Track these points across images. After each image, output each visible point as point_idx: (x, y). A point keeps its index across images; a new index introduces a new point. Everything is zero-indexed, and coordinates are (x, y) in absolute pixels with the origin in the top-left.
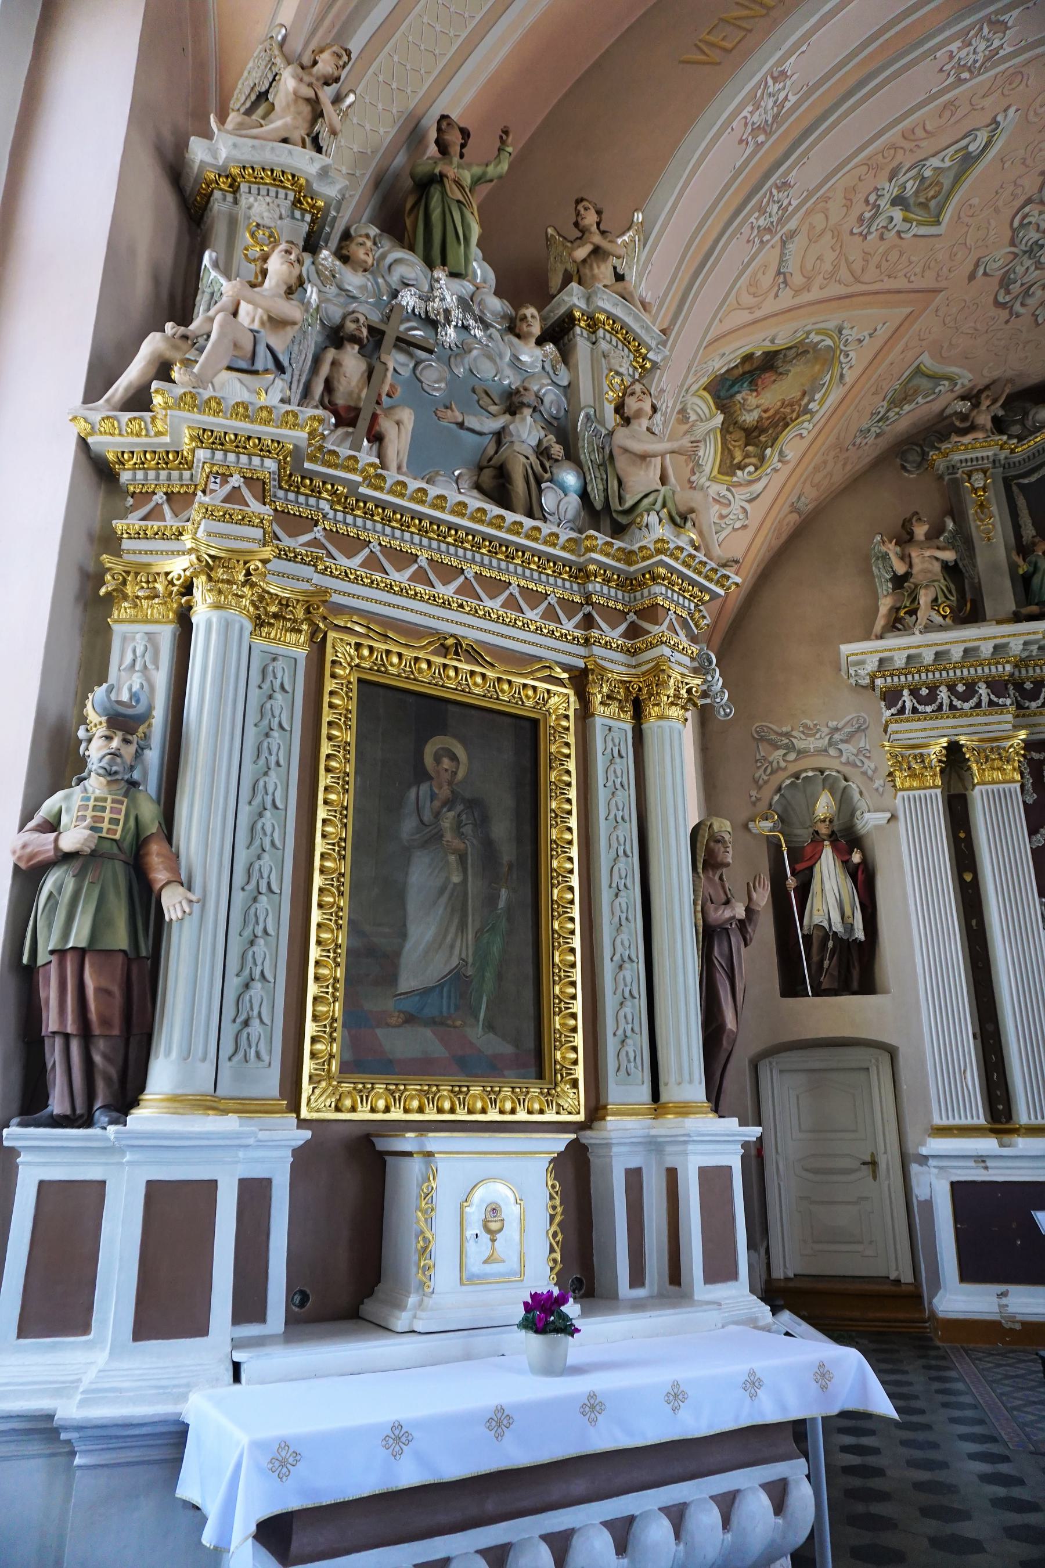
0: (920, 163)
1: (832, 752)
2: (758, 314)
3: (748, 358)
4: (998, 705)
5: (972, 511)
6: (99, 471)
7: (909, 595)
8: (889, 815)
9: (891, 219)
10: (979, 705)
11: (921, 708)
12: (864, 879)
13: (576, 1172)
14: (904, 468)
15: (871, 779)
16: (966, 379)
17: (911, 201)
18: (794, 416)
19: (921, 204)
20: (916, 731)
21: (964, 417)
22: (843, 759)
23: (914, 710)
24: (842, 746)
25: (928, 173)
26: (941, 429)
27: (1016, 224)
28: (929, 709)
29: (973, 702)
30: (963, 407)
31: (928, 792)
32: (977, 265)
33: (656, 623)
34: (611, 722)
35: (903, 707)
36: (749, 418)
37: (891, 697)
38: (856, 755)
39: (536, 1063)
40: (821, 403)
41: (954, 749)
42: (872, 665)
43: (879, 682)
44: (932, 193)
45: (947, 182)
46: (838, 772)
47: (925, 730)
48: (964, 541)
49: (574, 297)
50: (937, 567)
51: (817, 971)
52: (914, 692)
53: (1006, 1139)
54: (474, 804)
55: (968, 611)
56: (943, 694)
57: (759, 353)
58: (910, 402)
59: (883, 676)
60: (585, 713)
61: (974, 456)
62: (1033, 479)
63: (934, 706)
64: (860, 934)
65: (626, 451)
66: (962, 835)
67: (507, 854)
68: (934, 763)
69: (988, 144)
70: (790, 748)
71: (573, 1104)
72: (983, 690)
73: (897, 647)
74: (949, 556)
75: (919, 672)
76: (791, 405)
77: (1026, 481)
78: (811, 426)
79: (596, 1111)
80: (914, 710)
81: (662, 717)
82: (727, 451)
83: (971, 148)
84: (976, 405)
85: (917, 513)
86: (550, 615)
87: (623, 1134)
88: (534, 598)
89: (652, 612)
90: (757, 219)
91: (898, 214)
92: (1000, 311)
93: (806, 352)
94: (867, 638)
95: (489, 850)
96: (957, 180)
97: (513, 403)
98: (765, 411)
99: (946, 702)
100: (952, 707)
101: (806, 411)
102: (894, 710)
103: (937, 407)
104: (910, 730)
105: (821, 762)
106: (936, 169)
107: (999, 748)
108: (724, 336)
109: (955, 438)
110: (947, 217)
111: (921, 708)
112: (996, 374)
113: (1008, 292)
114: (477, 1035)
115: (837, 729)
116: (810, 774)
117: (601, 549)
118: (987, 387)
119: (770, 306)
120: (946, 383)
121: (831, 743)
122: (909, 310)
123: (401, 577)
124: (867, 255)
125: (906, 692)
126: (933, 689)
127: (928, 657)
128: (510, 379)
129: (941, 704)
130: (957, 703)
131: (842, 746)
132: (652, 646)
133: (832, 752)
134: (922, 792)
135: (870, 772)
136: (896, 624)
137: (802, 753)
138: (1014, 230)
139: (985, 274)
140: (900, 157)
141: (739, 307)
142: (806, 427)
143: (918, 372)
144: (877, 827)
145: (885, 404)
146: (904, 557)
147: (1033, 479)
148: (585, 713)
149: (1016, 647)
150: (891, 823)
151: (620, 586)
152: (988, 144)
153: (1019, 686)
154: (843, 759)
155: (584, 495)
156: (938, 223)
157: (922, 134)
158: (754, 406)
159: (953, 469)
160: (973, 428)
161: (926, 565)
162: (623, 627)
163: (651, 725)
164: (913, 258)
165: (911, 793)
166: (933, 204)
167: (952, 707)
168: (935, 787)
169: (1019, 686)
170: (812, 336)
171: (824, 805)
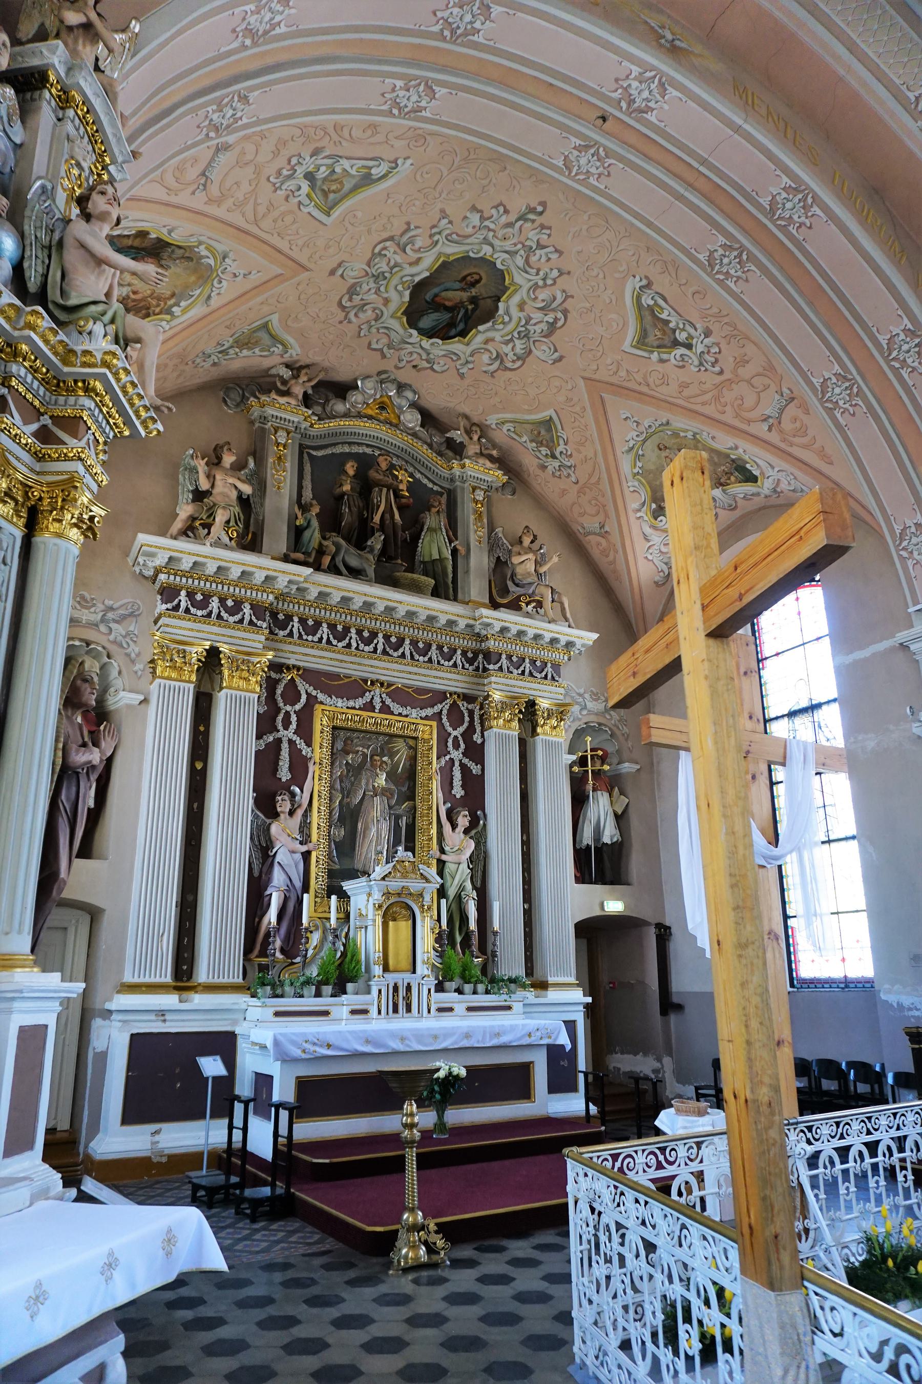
0: (336, 157)
1: (103, 628)
2: (173, 199)
3: (142, 234)
4: (256, 625)
5: (271, 460)
7: (208, 510)
8: (142, 698)
9: (299, 188)
10: (241, 621)
11: (193, 610)
14: (225, 401)
15: (133, 662)
16: (295, 352)
17: (319, 183)
18: (157, 310)
19: (323, 190)
20: (184, 629)
21: (285, 382)
22: (112, 637)
23: (187, 611)
24: (113, 626)
25: (338, 170)
26: (262, 384)
27: (377, 250)
28: (200, 613)
29: (237, 617)
30: (286, 373)
31: (182, 684)
32: (340, 265)
33: (75, 435)
35: (178, 605)
38: (124, 637)
40: (184, 311)
41: (213, 654)
42: (161, 560)
43: (162, 577)
44: (334, 187)
45: (348, 186)
46: (104, 648)
47: (192, 630)
48: (259, 481)
52: (190, 595)
53: (185, 995)
55: (250, 541)
56: (215, 604)
57: (153, 236)
58: (249, 349)
59: (169, 573)
61: (283, 416)
62: (320, 453)
63: (205, 612)
65: (82, 246)
66: (202, 728)
68: (194, 660)
69: (384, 176)
72: (247, 610)
73: (189, 551)
74: (247, 489)
75: (199, 579)
76: (159, 299)
77: (314, 453)
78: (167, 327)
80: (187, 611)
81: (59, 535)
83: (373, 171)
84: (296, 377)
85: (229, 443)
90: (214, 112)
91: (305, 187)
92: (339, 311)
93: (190, 259)
94: (163, 533)
96: (355, 189)
98: (135, 293)
99: (215, 611)
100: (219, 617)
101: (169, 312)
102: (169, 606)
103: (266, 363)
104: (180, 627)
105: (90, 635)
106: (345, 170)
107: (249, 661)
108: (139, 200)
109: (273, 395)
110: (337, 213)
111: (193, 610)
112: (317, 359)
113: (350, 300)
115: (111, 609)
116: (77, 643)
118: (307, 366)
119: (184, 198)
120: (280, 347)
121: (103, 620)
122: (280, 271)
124: (271, 206)
125: (183, 593)
126: (207, 597)
127: (211, 568)
129: (211, 612)
130: (225, 615)
131: (113, 626)
132: (67, 459)
133: (103, 628)
134: (177, 684)
135: (133, 655)
138: (373, 254)
139: (342, 276)
140: (325, 142)
141: (161, 181)
143: (265, 326)
144: (129, 706)
145: (231, 340)
146: (210, 477)
147: (320, 453)
149: (281, 583)
150: (143, 705)
151: (44, 382)
152: (384, 176)
153: (274, 615)
154: (112, 637)
156: (328, 214)
157: (347, 136)
159: (264, 419)
160: (287, 393)
161: (226, 490)
162: (35, 427)
163: (43, 540)
164: (301, 231)
165: (168, 682)
166: (332, 196)
167: (219, 617)
168: (189, 682)
169: (274, 615)
170: (202, 247)
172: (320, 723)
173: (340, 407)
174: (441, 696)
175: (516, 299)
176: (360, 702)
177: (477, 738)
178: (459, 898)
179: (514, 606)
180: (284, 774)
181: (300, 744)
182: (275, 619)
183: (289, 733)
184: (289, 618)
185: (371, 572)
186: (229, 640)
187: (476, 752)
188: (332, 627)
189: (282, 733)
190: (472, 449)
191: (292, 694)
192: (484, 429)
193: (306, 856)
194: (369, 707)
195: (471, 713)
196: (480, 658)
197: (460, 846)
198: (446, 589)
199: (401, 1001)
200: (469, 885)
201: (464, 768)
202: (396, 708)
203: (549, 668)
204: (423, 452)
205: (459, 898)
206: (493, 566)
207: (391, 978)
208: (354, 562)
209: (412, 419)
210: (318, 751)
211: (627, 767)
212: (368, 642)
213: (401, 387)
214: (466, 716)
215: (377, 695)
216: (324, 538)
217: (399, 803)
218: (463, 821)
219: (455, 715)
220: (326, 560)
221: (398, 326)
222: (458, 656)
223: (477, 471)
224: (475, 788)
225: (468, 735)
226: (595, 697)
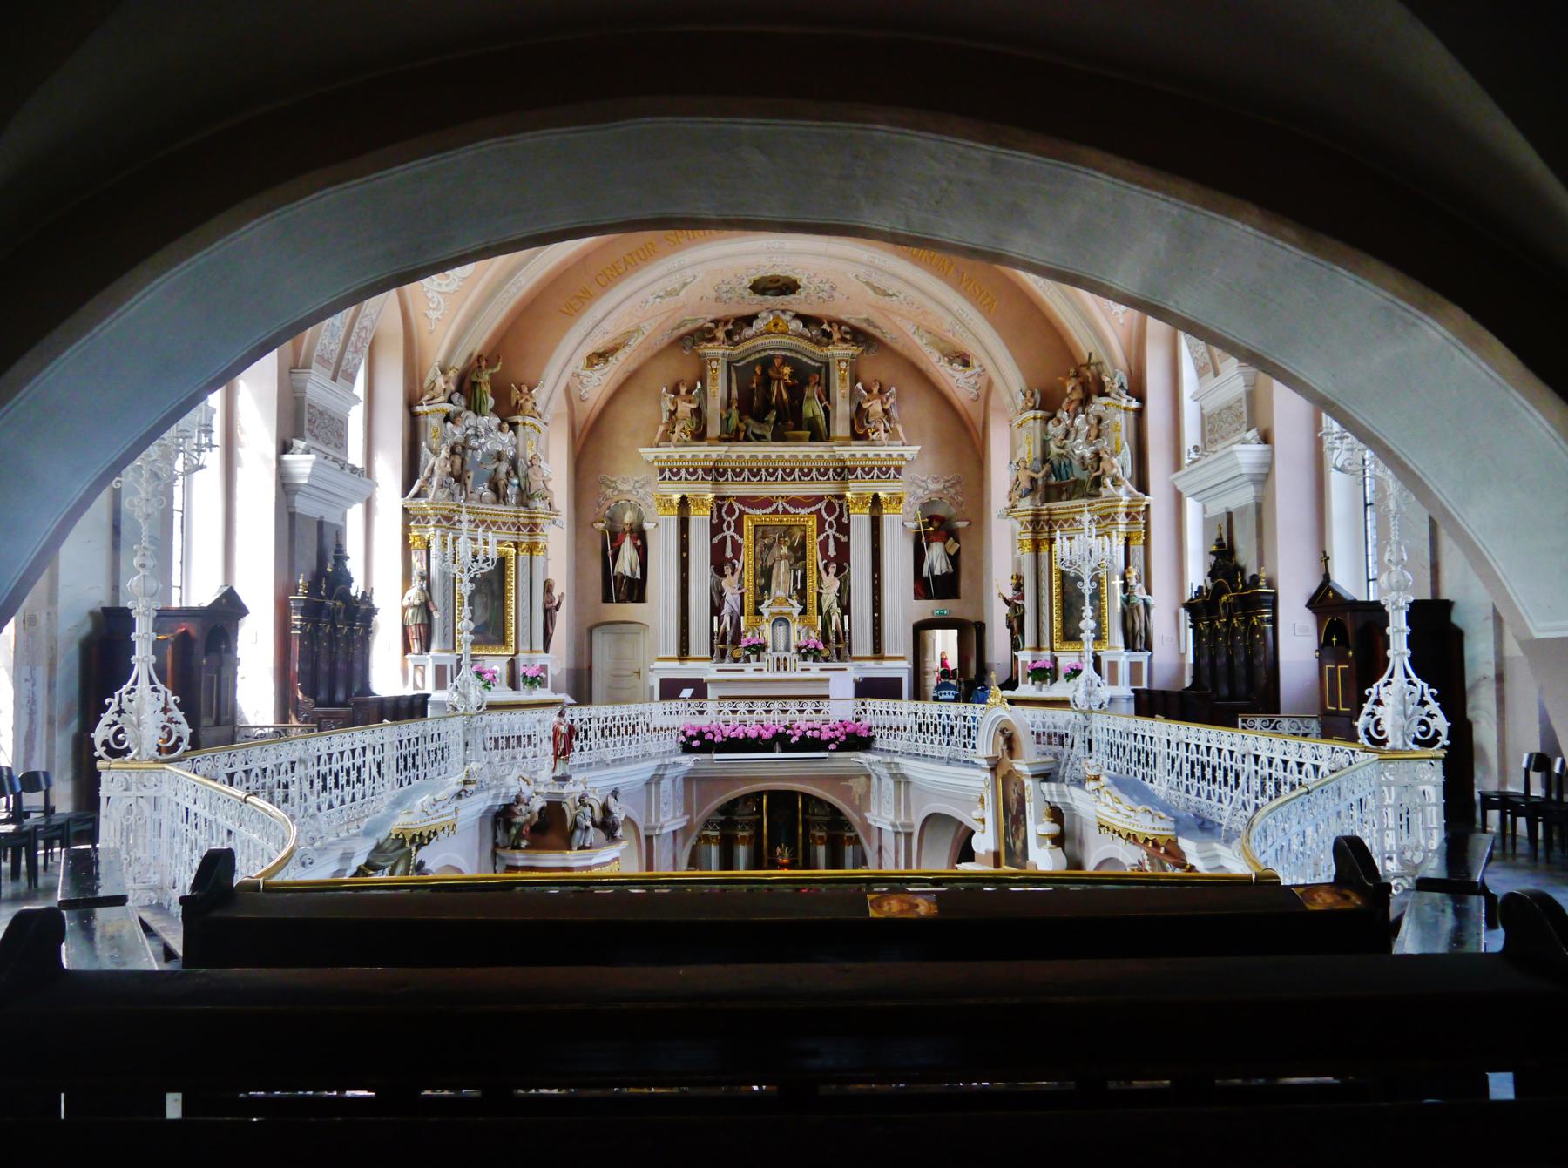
6: (405, 510)
13: (512, 664)
16: (711, 317)
26: (703, 335)
30: (712, 325)
34: (524, 555)
37: (662, 470)
39: (503, 641)
41: (684, 498)
42: (651, 458)
49: (519, 419)
51: (618, 591)
56: (683, 472)
64: (638, 576)
70: (615, 488)
71: (512, 651)
72: (700, 472)
73: (664, 452)
79: (517, 652)
87: (523, 657)
89: (536, 525)
97: (499, 457)
114: (490, 635)
126: (679, 469)
136: (666, 438)
137: (621, 492)
142: (628, 349)
146: (674, 403)
149: (714, 456)
171: (628, 518)
172: (748, 525)
173: (748, 332)
174: (820, 498)
176: (770, 510)
177: (845, 520)
178: (828, 612)
179: (865, 437)
180: (729, 554)
181: (737, 537)
182: (716, 472)
183: (731, 532)
184: (725, 470)
185: (769, 436)
186: (688, 489)
187: (844, 529)
188: (750, 470)
189: (729, 533)
190: (836, 336)
191: (731, 511)
192: (840, 323)
193: (742, 595)
194: (776, 512)
195: (841, 506)
196: (844, 472)
197: (832, 584)
198: (819, 434)
199: (782, 664)
200: (835, 605)
201: (836, 540)
202: (792, 510)
203: (892, 471)
204: (805, 345)
205: (828, 612)
206: (854, 408)
207: (775, 655)
208: (758, 432)
209: (797, 325)
210: (747, 541)
211: (961, 524)
212: (771, 475)
213: (783, 311)
214: (836, 508)
215: (780, 505)
216: (741, 420)
217: (797, 561)
218: (833, 569)
219: (830, 509)
220: (742, 435)
221: (758, 297)
222: (831, 472)
223: (839, 352)
224: (843, 551)
225: (838, 520)
226: (936, 480)
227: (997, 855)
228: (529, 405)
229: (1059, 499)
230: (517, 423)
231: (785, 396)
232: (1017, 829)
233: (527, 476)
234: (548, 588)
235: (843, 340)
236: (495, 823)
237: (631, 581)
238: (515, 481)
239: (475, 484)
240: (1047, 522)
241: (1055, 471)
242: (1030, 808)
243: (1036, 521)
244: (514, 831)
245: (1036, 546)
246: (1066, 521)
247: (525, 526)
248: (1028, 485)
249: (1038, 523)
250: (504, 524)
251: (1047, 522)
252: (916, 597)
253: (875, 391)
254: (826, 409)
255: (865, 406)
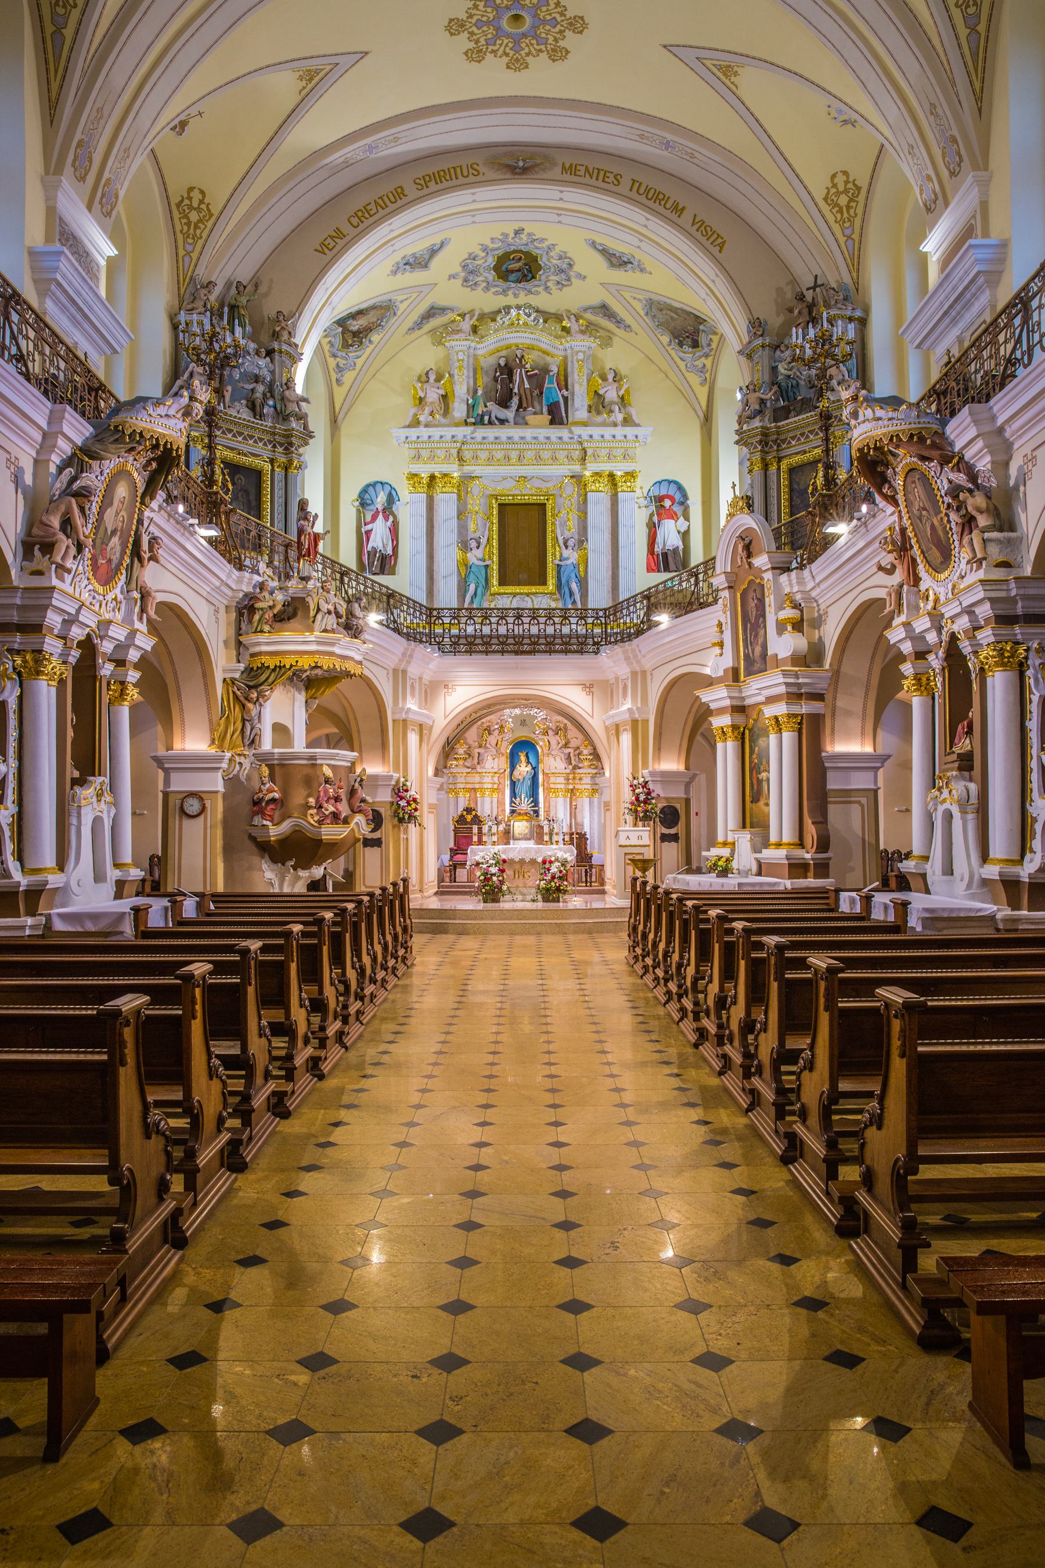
12: (394, 531)
36: (355, 328)
41: (432, 478)
50: (436, 396)
54: (246, 491)
60: (273, 470)
64: (390, 551)
67: (254, 503)
74: (442, 392)
82: (344, 339)
86: (265, 444)
88: (261, 440)
89: (291, 444)
95: (249, 501)
97: (257, 379)
117: (280, 427)
123: (230, 436)
128: (256, 371)
148: (273, 470)
155: (275, 408)
158: (355, 325)
175: (544, 259)
185: (512, 420)
208: (501, 416)
227: (735, 671)
228: (285, 336)
229: (787, 418)
230: (273, 351)
231: (527, 386)
232: (756, 635)
233: (283, 399)
234: (303, 505)
235: (583, 332)
236: (240, 614)
237: (384, 558)
238: (271, 403)
239: (233, 400)
240: (775, 442)
241: (783, 392)
242: (770, 600)
243: (764, 443)
244: (257, 617)
245: (766, 467)
246: (793, 438)
247: (281, 445)
248: (757, 407)
249: (767, 444)
250: (261, 440)
251: (775, 442)
252: (648, 571)
253: (610, 377)
254: (566, 399)
255: (601, 392)
